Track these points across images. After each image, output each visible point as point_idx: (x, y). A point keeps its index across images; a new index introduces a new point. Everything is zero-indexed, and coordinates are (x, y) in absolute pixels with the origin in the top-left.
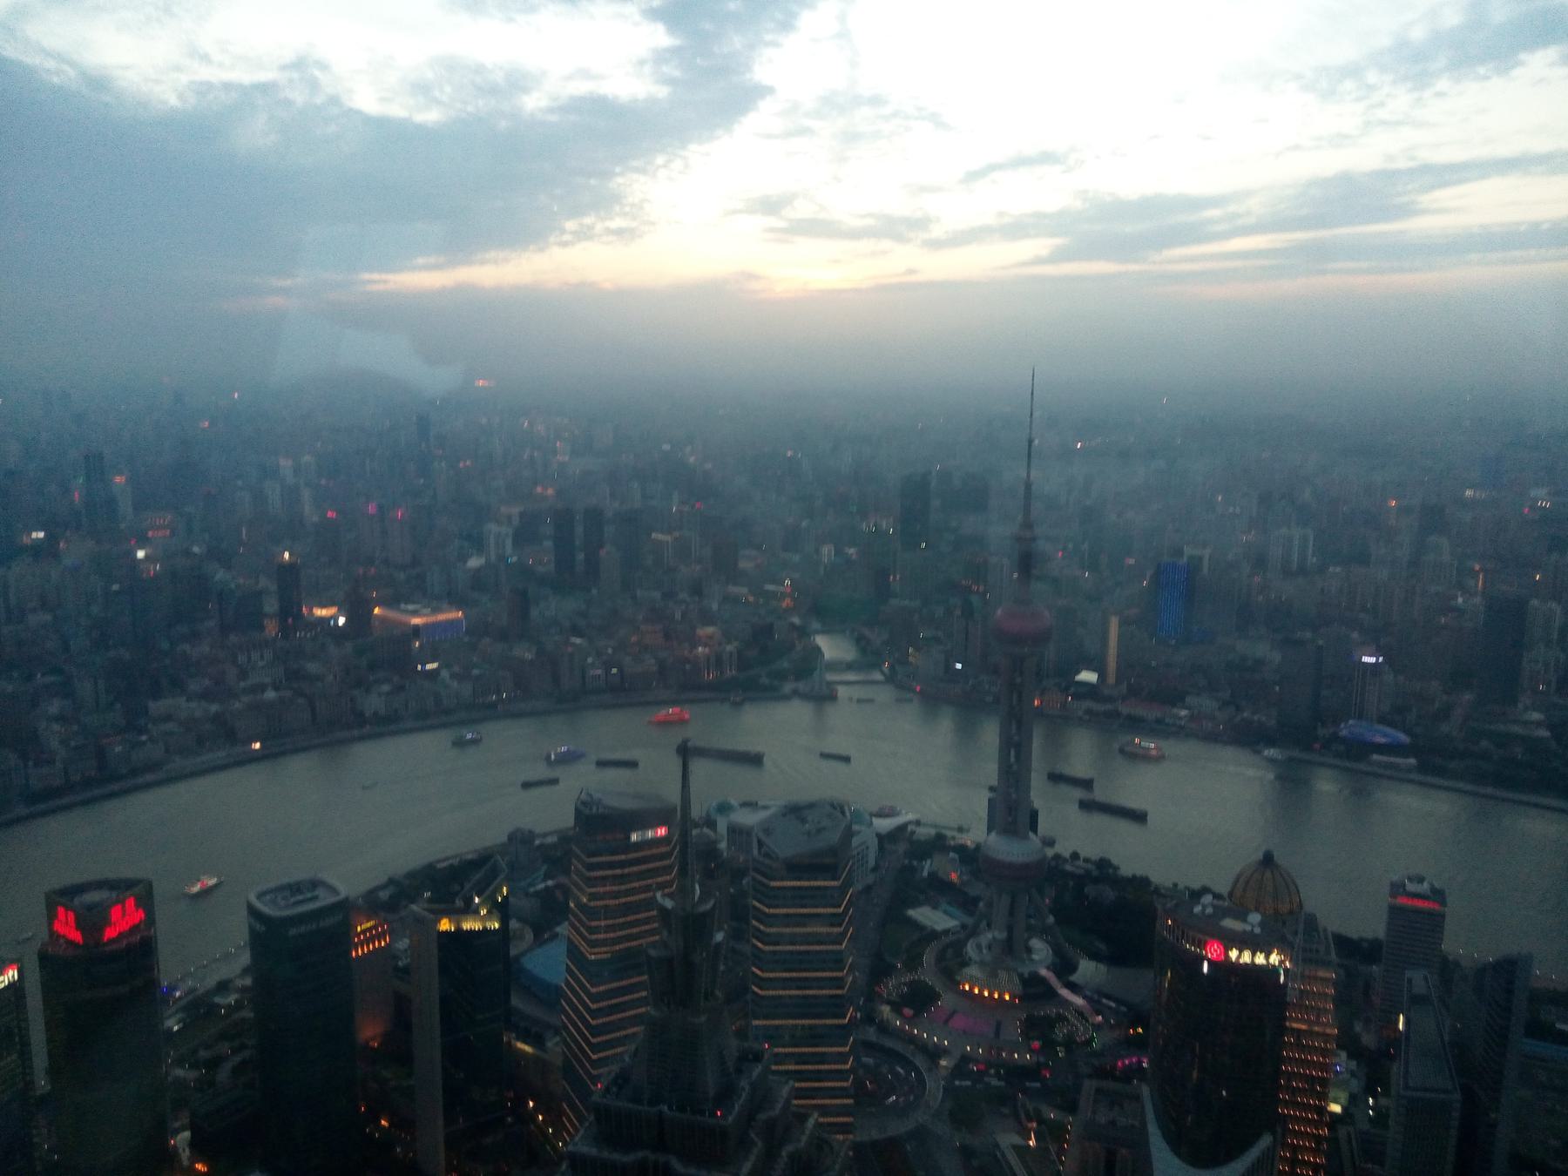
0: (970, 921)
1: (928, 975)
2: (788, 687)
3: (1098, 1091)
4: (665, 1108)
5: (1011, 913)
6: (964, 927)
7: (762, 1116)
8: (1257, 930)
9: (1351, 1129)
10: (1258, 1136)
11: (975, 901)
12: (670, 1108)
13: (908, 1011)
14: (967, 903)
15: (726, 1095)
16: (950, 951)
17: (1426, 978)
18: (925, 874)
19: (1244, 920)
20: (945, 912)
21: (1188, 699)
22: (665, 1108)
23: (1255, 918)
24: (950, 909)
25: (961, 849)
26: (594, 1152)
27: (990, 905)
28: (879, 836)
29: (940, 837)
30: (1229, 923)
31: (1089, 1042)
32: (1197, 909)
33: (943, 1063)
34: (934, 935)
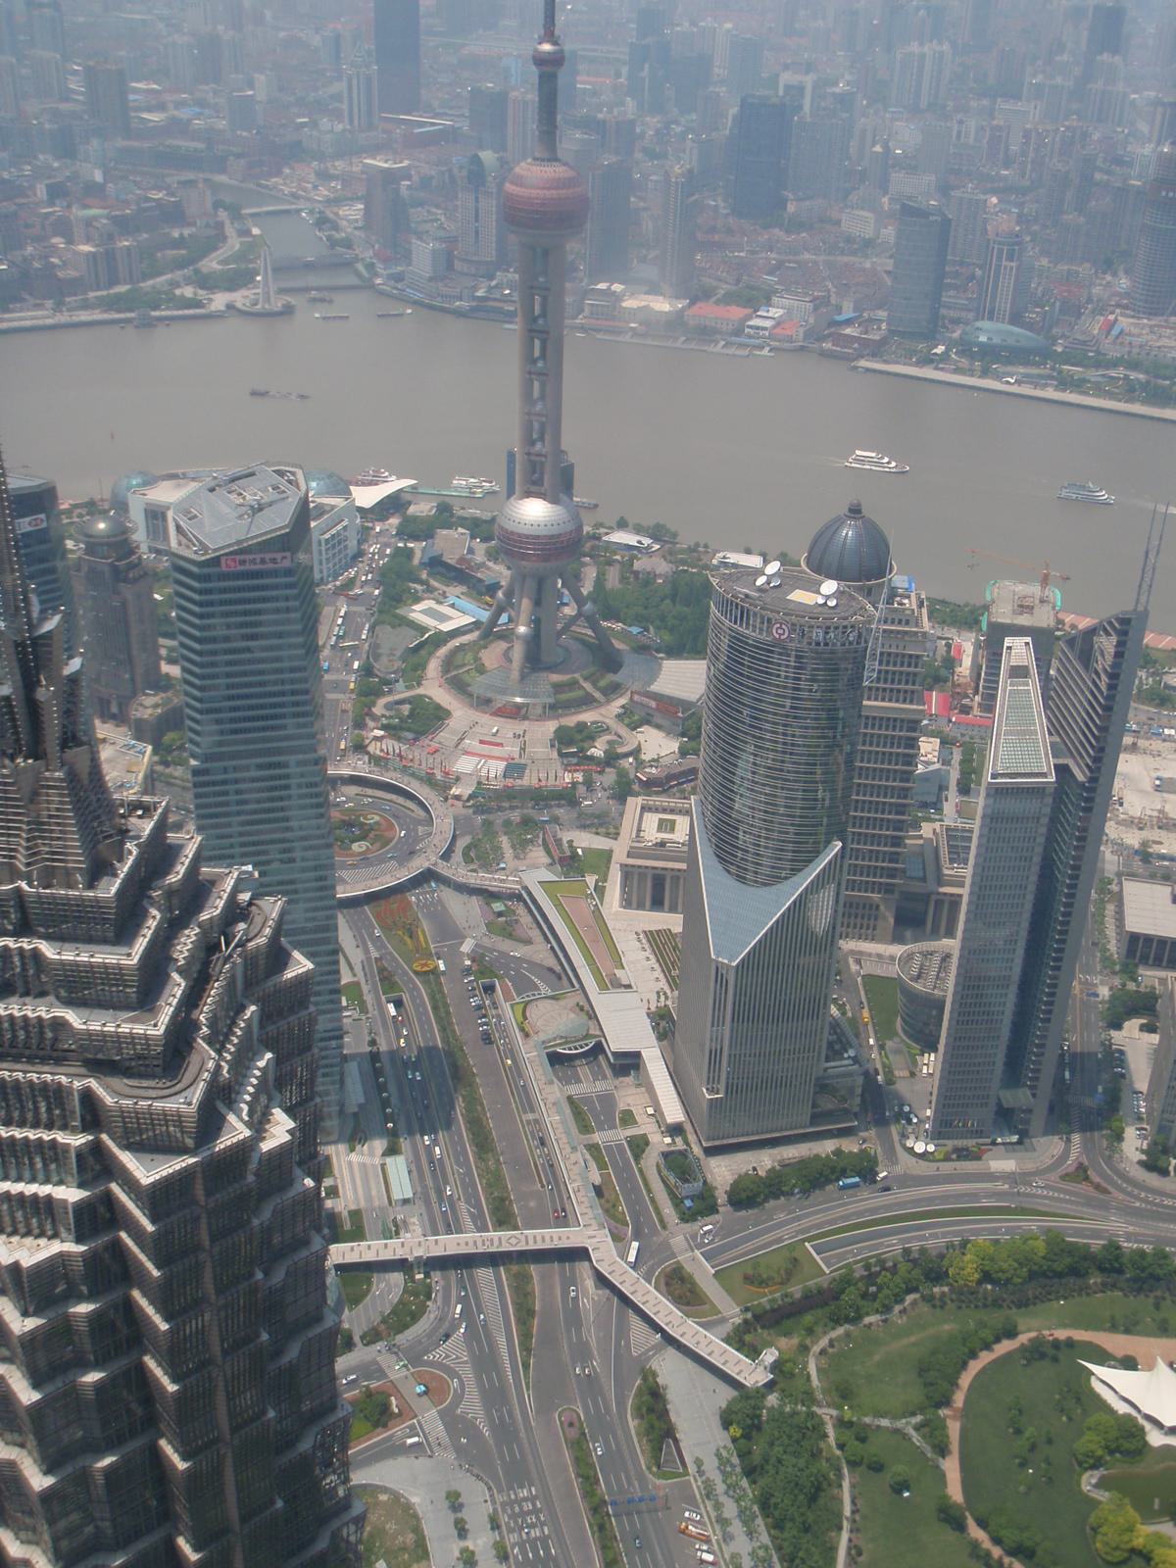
1: (434, 689)
2: (219, 301)
3: (645, 809)
4: (24, 885)
6: (477, 625)
8: (832, 603)
10: (828, 842)
11: (492, 589)
12: (30, 885)
13: (410, 735)
14: (482, 590)
16: (459, 657)
17: (1027, 644)
18: (426, 560)
19: (818, 592)
20: (453, 606)
21: (775, 299)
22: (24, 885)
23: (830, 587)
24: (458, 602)
28: (360, 509)
29: (444, 509)
30: (799, 596)
33: (455, 791)
34: (441, 638)
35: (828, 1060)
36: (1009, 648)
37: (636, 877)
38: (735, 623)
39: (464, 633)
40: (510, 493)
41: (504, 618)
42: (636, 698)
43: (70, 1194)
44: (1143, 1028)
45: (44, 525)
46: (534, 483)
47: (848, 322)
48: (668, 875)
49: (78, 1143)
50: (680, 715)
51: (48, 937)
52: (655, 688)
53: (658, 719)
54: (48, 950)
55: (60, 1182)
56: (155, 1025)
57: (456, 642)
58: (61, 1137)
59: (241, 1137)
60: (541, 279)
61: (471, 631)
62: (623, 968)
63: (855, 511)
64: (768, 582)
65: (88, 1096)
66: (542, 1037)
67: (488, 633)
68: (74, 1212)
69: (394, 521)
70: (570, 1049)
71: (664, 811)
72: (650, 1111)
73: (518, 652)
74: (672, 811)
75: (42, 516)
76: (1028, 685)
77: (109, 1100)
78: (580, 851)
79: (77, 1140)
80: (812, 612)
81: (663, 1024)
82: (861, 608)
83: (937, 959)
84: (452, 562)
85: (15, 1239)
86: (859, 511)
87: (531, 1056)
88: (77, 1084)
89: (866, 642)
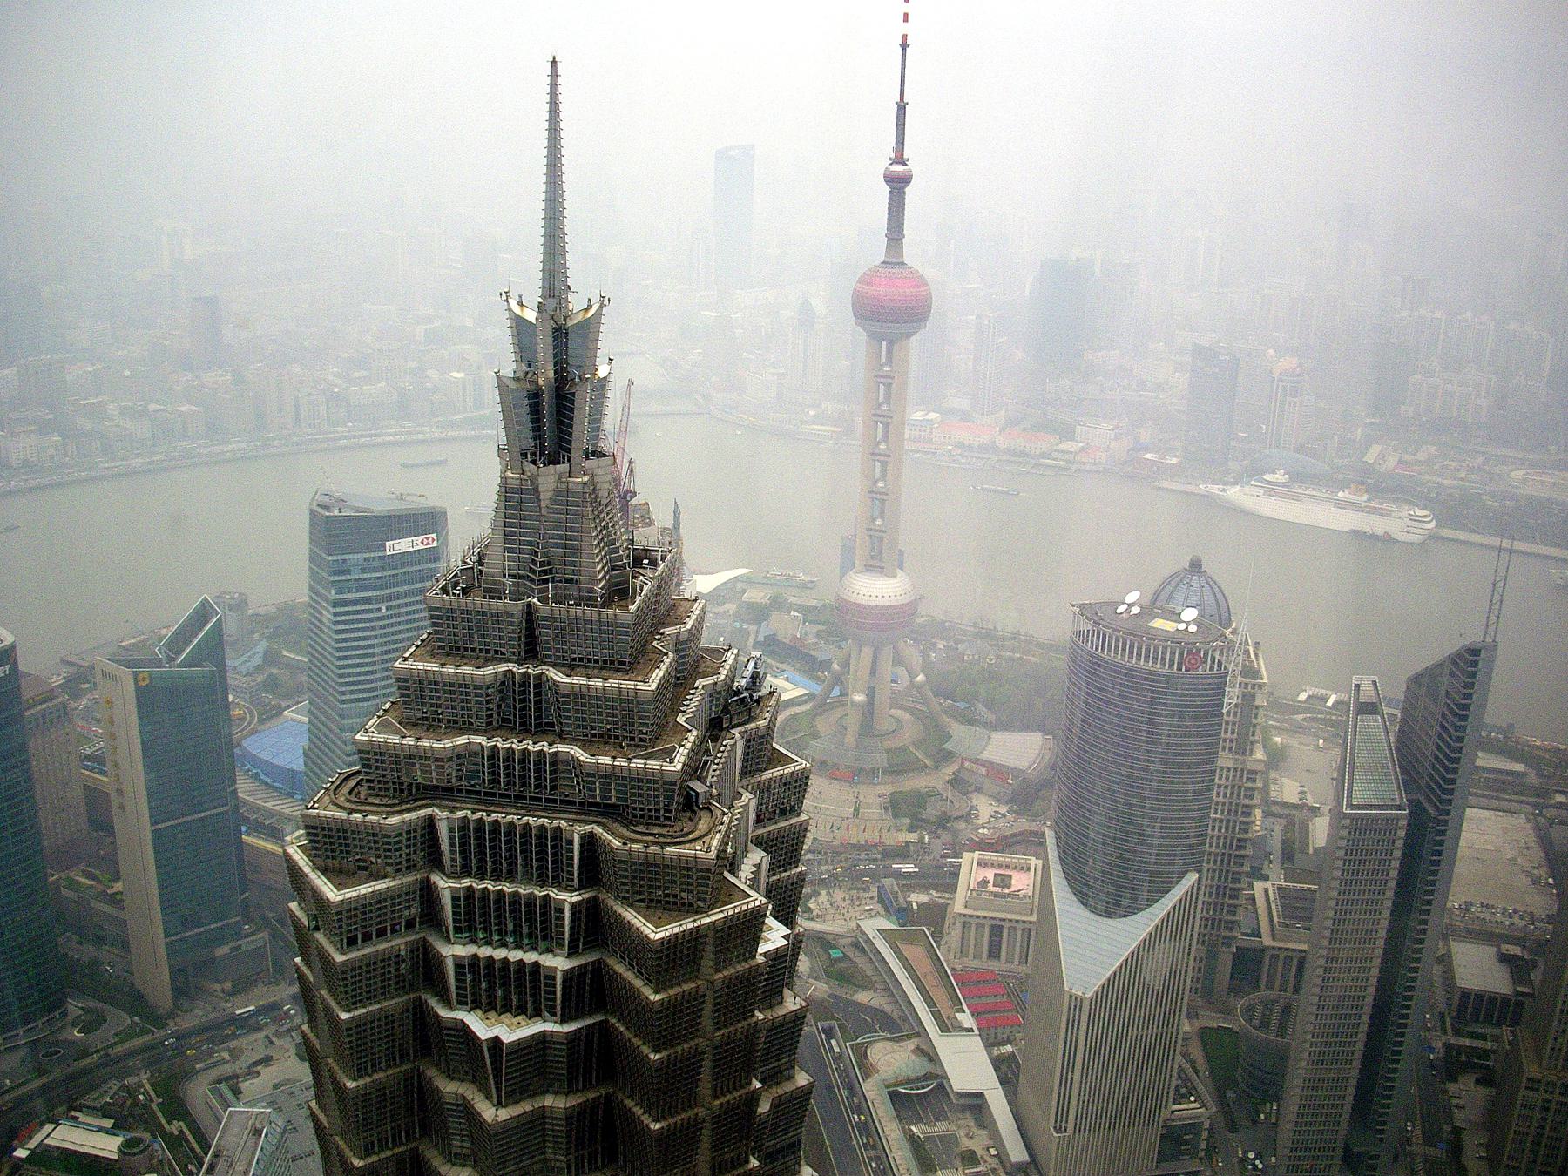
0: (817, 689)
5: (873, 673)
6: (810, 697)
7: (670, 631)
8: (1193, 628)
9: (1268, 884)
10: (1182, 874)
11: (825, 666)
12: (544, 600)
15: (620, 592)
17: (1374, 683)
18: (761, 638)
20: (787, 679)
22: (536, 600)
25: (805, 610)
26: (434, 667)
27: (846, 664)
31: (967, 818)
32: (1121, 609)
35: (1174, 1104)
36: (1357, 686)
37: (973, 929)
38: (1097, 649)
39: (798, 704)
40: (847, 566)
41: (836, 691)
42: (967, 764)
43: (558, 963)
44: (1478, 1082)
45: (435, 544)
46: (872, 557)
47: (1147, 450)
48: (1006, 925)
49: (574, 899)
50: (1010, 781)
51: (555, 665)
52: (984, 756)
53: (988, 784)
54: (557, 676)
55: (549, 951)
56: (672, 761)
57: (791, 711)
58: (555, 894)
59: (758, 903)
60: (886, 369)
61: (806, 702)
62: (964, 1012)
63: (1196, 566)
64: (1128, 611)
65: (590, 841)
66: (883, 1075)
67: (822, 705)
68: (564, 982)
69: (731, 607)
70: (912, 1089)
71: (1000, 867)
72: (993, 1151)
73: (853, 721)
74: (1008, 867)
75: (434, 536)
76: (1377, 721)
77: (616, 843)
78: (915, 906)
79: (568, 898)
80: (1177, 638)
81: (1007, 1071)
82: (1221, 636)
83: (1278, 1007)
84: (787, 641)
85: (492, 1015)
86: (1200, 566)
87: (872, 1090)
88: (579, 828)
89: (1226, 668)
